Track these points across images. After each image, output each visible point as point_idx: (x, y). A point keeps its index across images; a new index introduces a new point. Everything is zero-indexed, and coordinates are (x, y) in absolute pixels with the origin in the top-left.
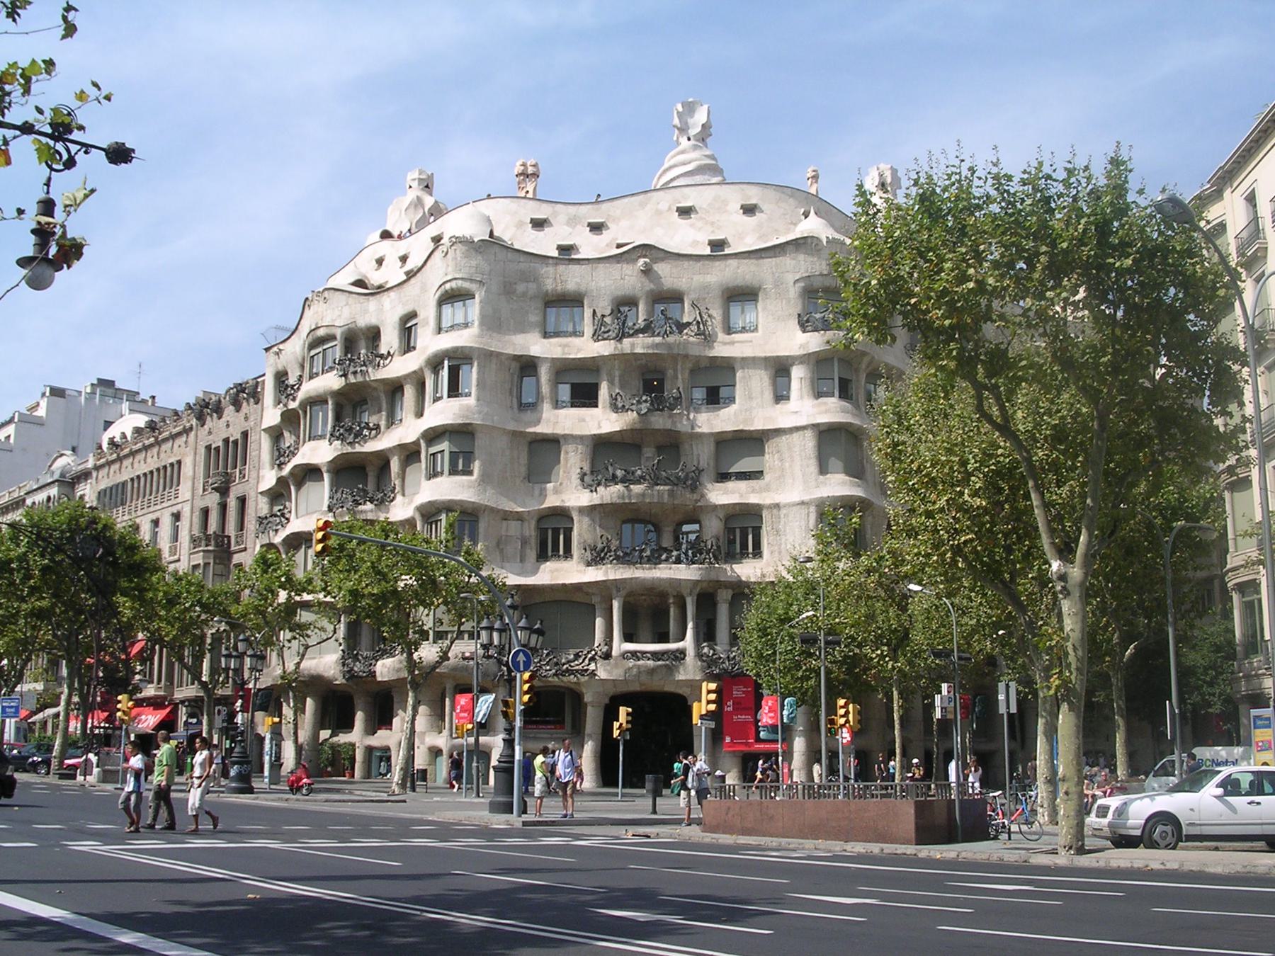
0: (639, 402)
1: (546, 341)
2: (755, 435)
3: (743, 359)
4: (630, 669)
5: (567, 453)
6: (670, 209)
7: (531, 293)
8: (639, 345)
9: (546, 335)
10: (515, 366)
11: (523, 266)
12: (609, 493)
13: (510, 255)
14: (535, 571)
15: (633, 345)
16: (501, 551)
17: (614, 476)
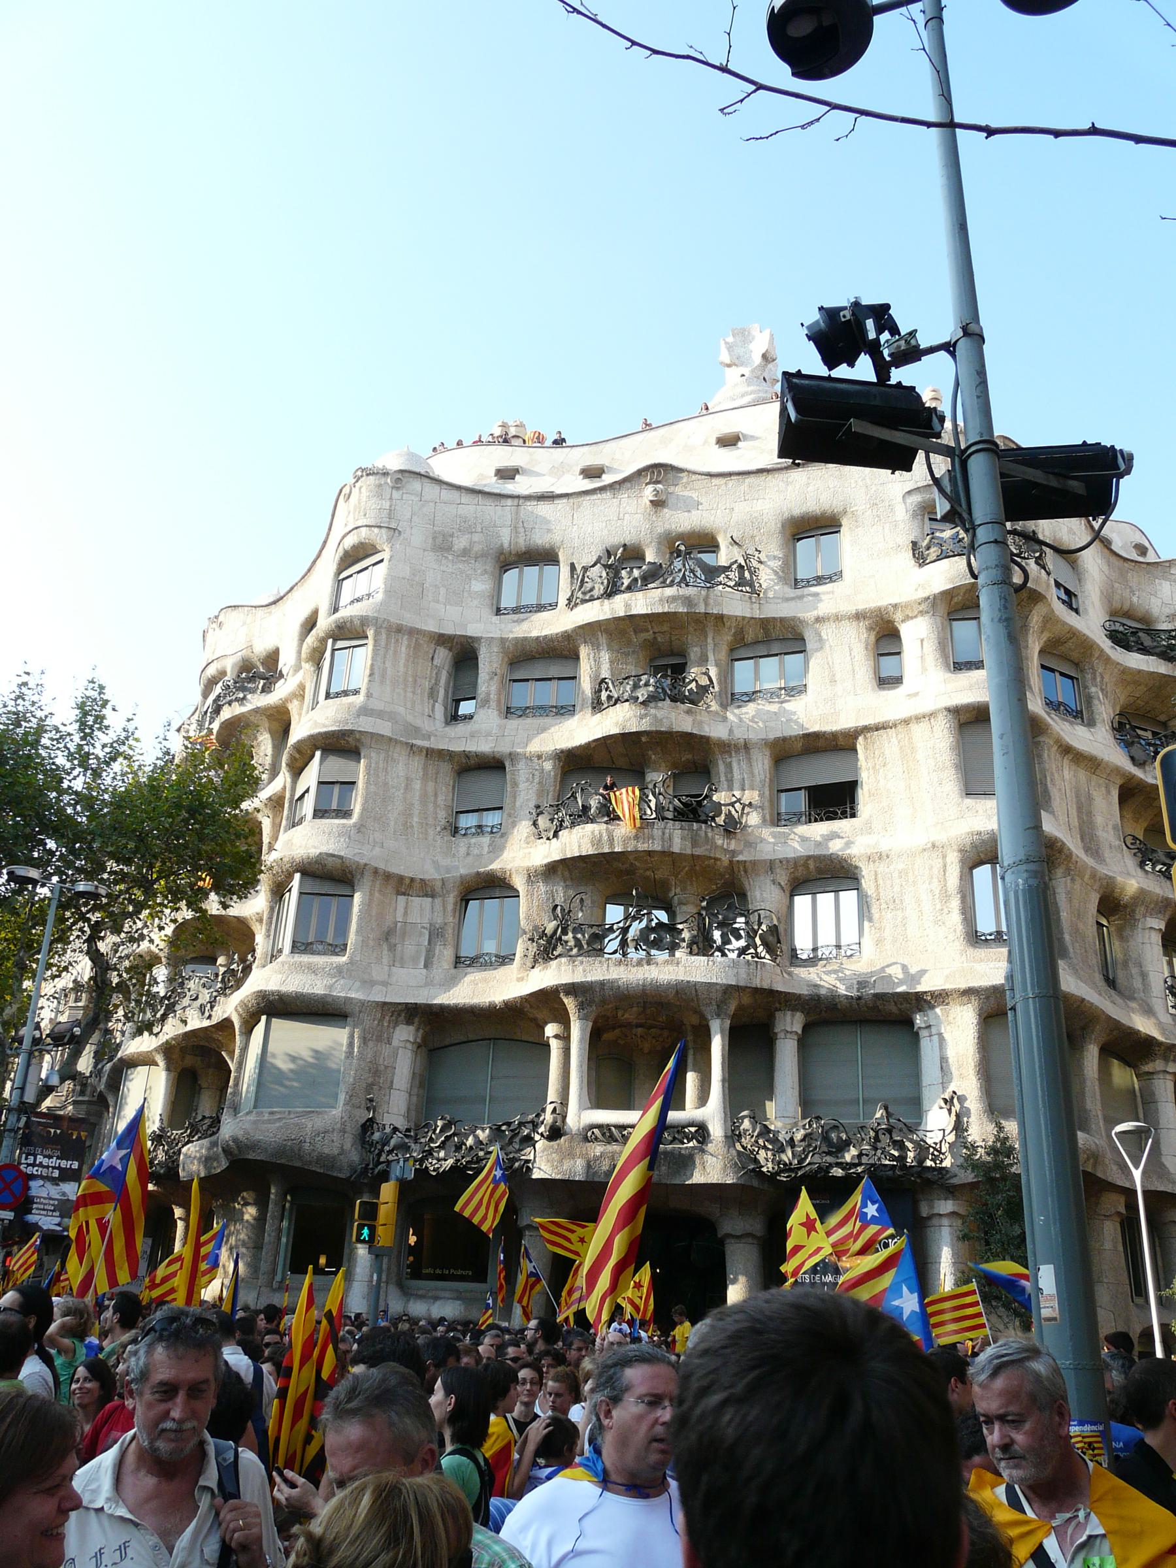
0: (636, 687)
1: (495, 619)
2: (841, 742)
3: (818, 620)
4: (596, 1159)
5: (515, 784)
6: (706, 442)
7: (477, 548)
8: (642, 603)
9: (498, 611)
10: (443, 656)
11: (462, 510)
12: (578, 841)
13: (444, 492)
14: (451, 982)
15: (627, 606)
16: (392, 948)
17: (586, 808)
